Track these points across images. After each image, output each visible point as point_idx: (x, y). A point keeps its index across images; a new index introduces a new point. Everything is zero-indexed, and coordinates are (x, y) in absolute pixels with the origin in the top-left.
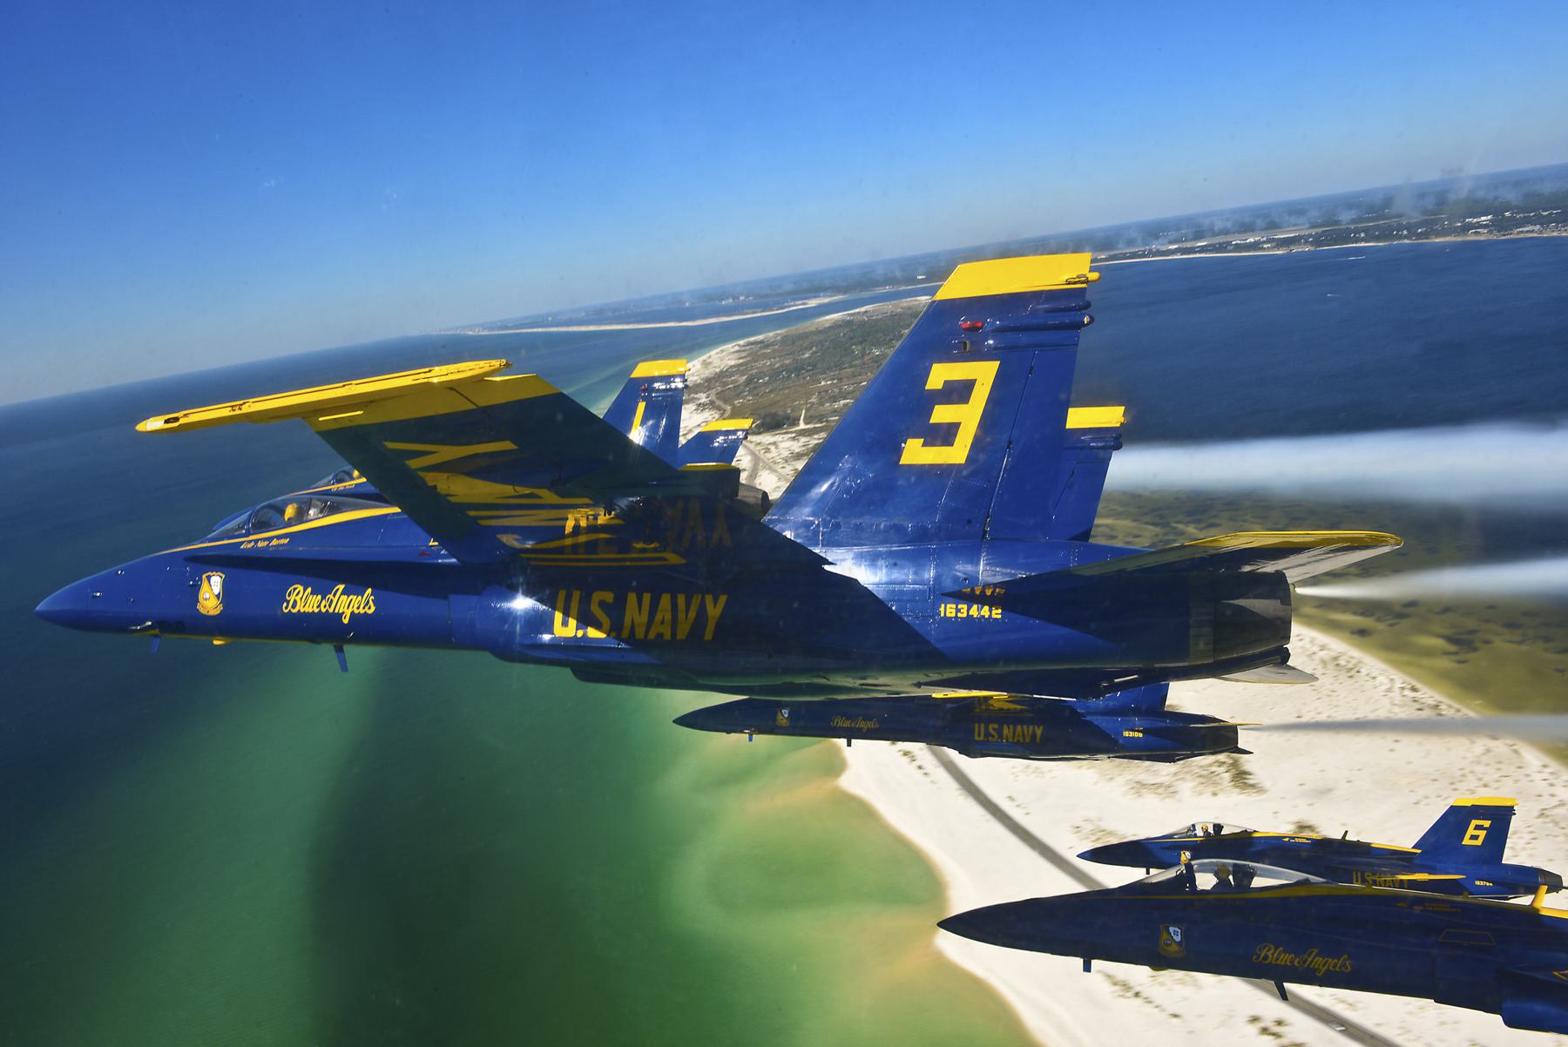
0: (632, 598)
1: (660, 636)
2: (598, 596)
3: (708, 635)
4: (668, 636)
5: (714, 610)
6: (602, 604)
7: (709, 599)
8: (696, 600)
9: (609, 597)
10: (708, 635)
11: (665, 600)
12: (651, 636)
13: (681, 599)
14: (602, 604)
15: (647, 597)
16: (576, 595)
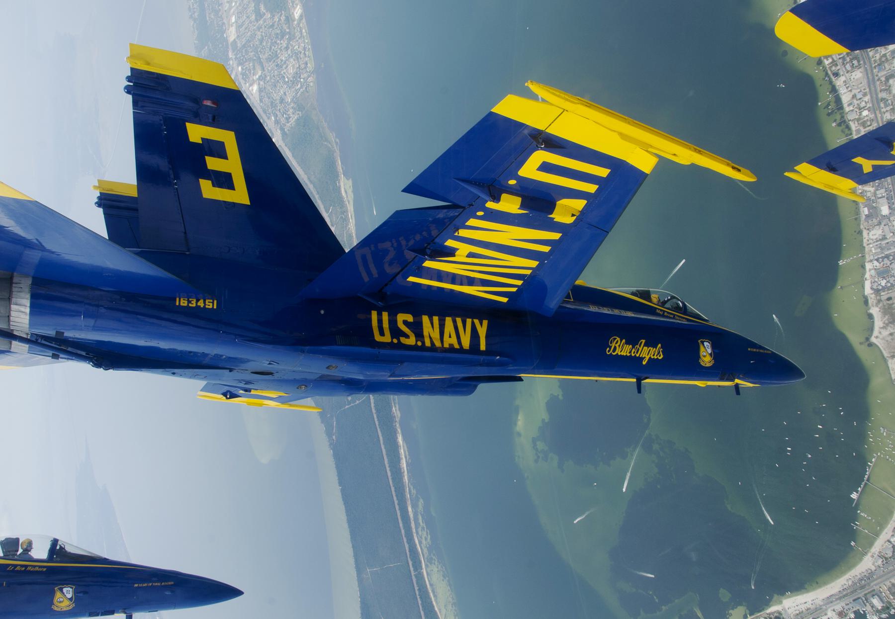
0: (425, 319)
1: (451, 345)
2: (401, 317)
3: (483, 347)
4: (457, 346)
5: (482, 331)
6: (405, 322)
7: (476, 321)
8: (469, 321)
9: (410, 318)
10: (483, 347)
11: (449, 321)
12: (446, 345)
13: (459, 320)
14: (405, 322)
15: (436, 319)
16: (385, 316)
